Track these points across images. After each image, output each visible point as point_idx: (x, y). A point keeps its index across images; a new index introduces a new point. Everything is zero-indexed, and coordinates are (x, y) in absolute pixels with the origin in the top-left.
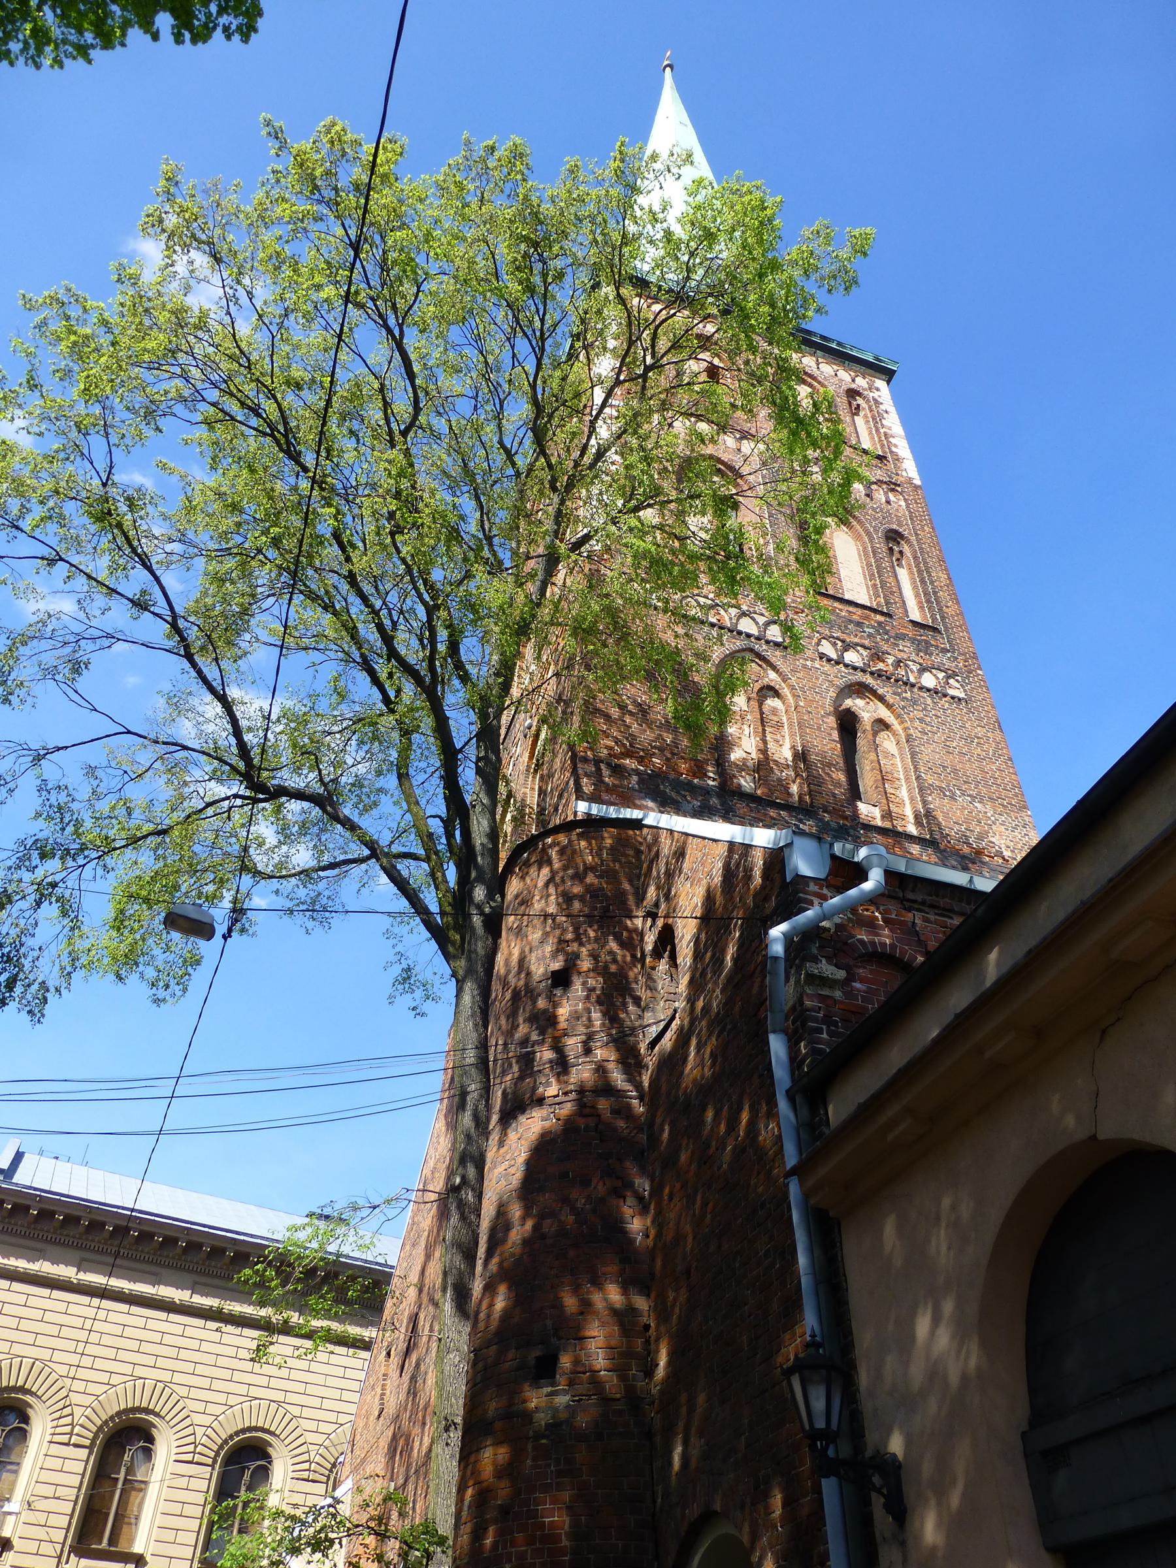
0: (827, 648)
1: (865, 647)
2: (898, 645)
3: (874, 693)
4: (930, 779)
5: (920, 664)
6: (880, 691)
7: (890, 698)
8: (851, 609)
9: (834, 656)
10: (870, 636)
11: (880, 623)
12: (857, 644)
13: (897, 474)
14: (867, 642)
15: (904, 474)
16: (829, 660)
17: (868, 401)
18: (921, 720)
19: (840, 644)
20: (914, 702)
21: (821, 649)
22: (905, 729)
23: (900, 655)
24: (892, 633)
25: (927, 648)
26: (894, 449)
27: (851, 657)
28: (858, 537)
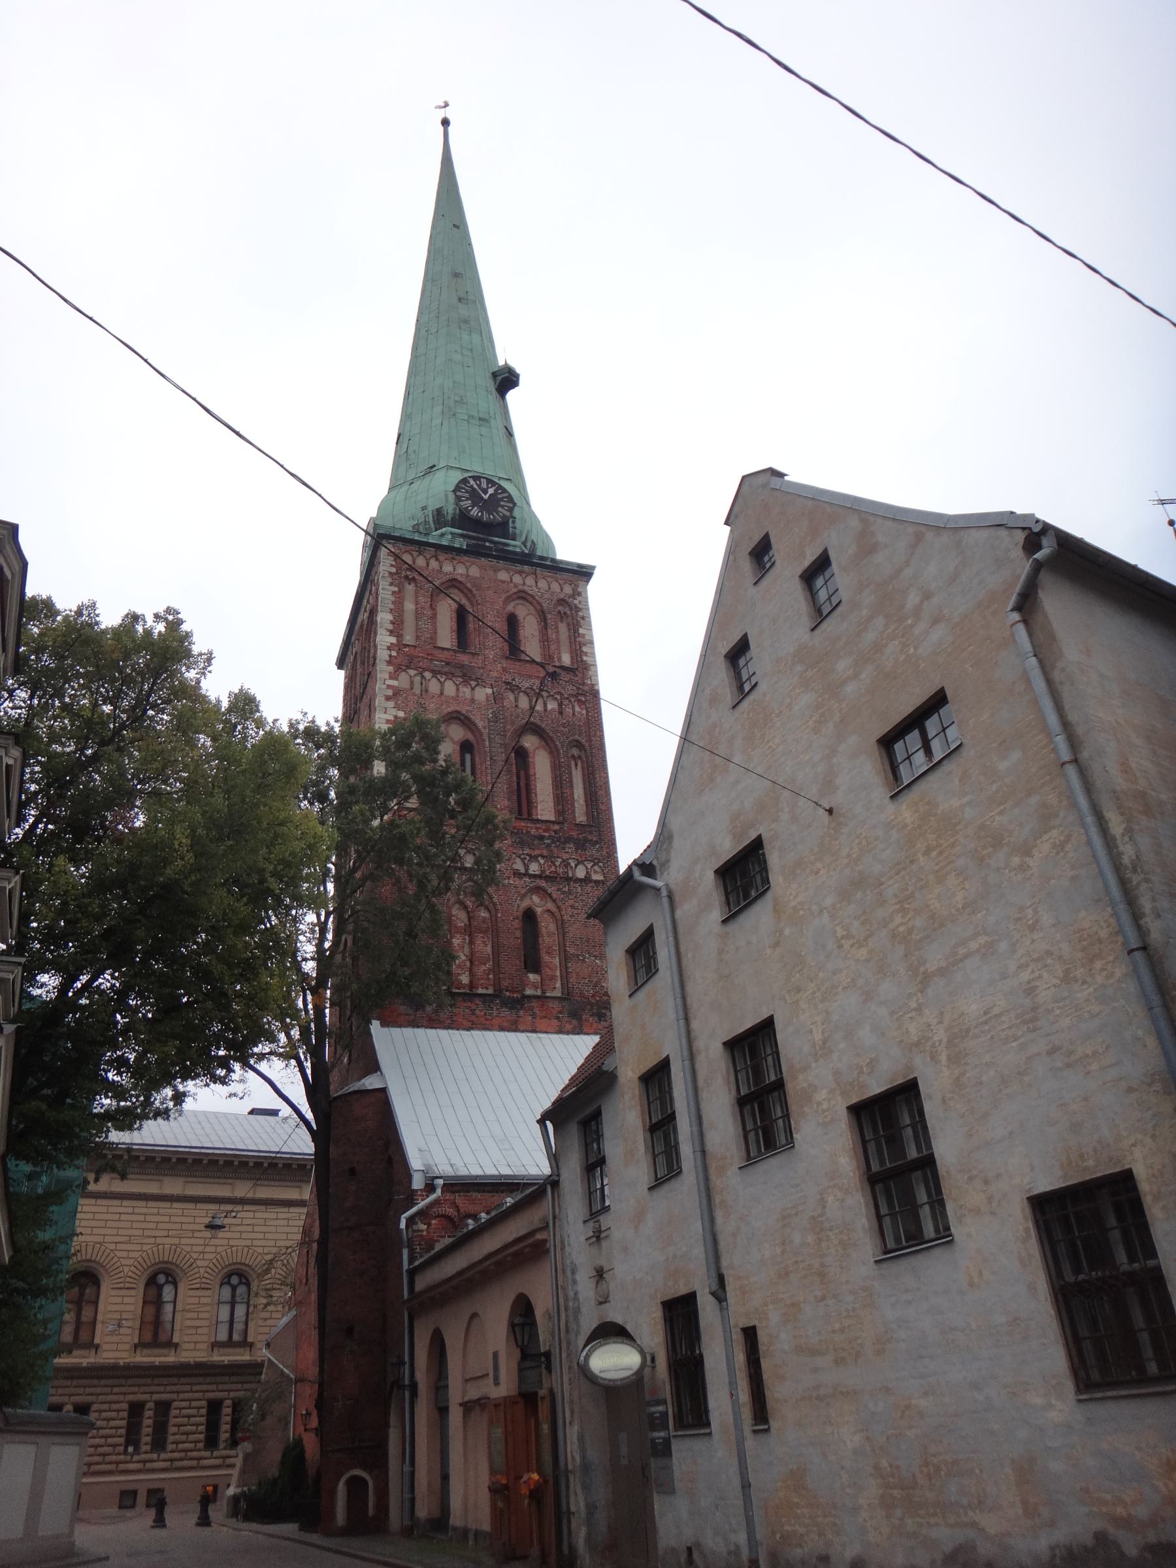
0: (519, 866)
1: (543, 857)
2: (564, 849)
3: (545, 891)
4: (571, 950)
5: (577, 860)
6: (549, 891)
7: (554, 896)
8: (538, 826)
9: (523, 871)
10: (548, 845)
11: (556, 832)
12: (539, 856)
13: (584, 684)
14: (545, 853)
15: (589, 682)
16: (520, 874)
17: (571, 609)
18: (572, 907)
19: (528, 858)
20: (570, 892)
21: (516, 867)
22: (562, 916)
23: (565, 856)
24: (562, 840)
25: (584, 845)
26: (585, 658)
27: (534, 868)
28: (551, 753)
